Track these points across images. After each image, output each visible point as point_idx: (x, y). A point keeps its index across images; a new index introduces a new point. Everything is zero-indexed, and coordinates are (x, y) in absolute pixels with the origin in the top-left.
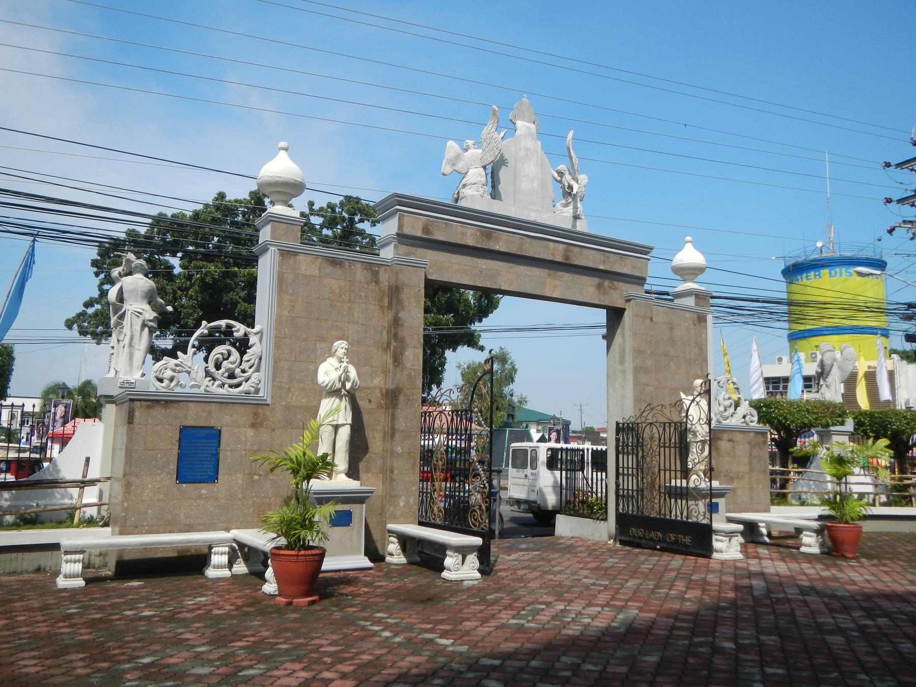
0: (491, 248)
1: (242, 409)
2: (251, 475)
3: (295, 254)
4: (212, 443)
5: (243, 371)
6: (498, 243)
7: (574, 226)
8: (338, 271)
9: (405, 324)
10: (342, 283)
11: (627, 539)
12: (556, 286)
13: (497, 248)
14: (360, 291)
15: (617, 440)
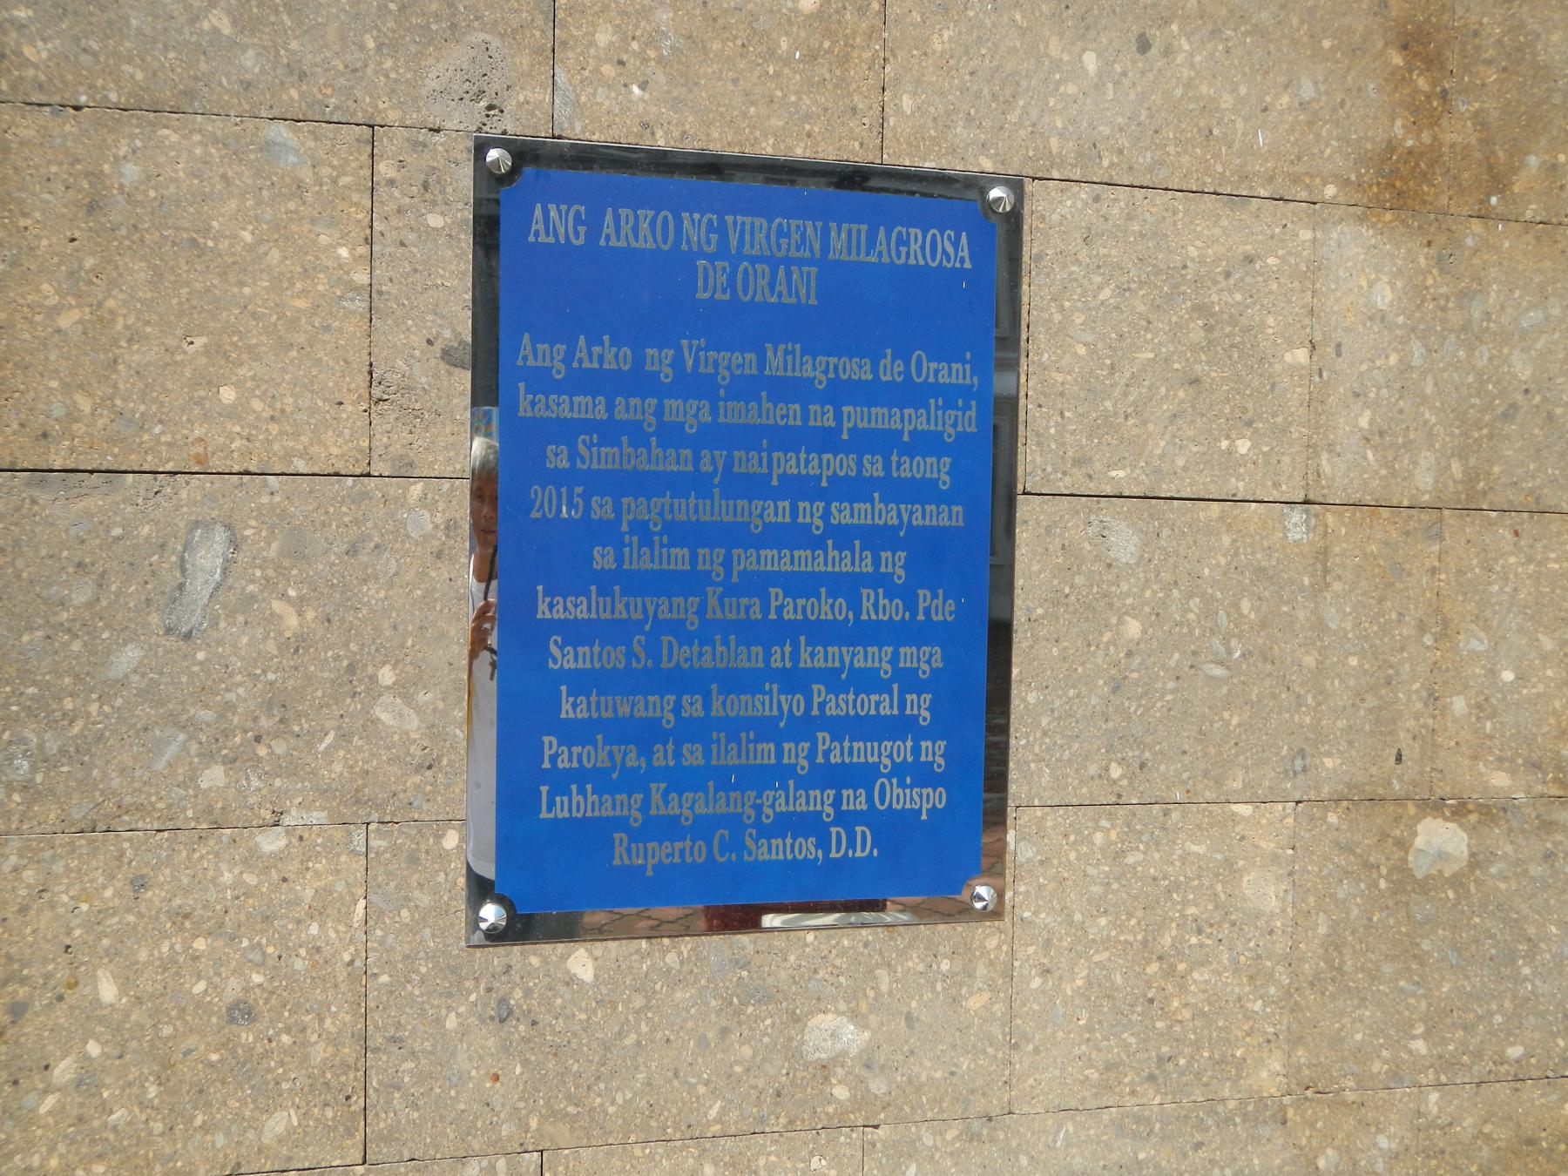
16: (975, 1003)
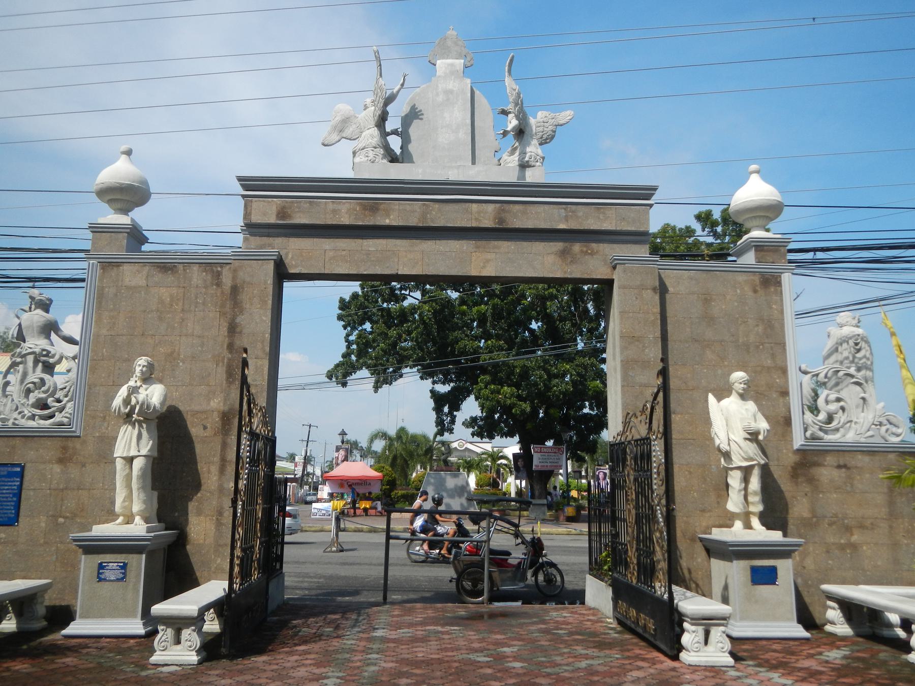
0: (378, 223)
1: (49, 443)
2: (55, 517)
3: (118, 265)
4: (14, 481)
5: (59, 401)
6: (388, 216)
7: (522, 176)
8: (170, 278)
9: (245, 331)
10: (174, 291)
12: (488, 261)
13: (387, 222)
14: (196, 298)
16: (15, 533)
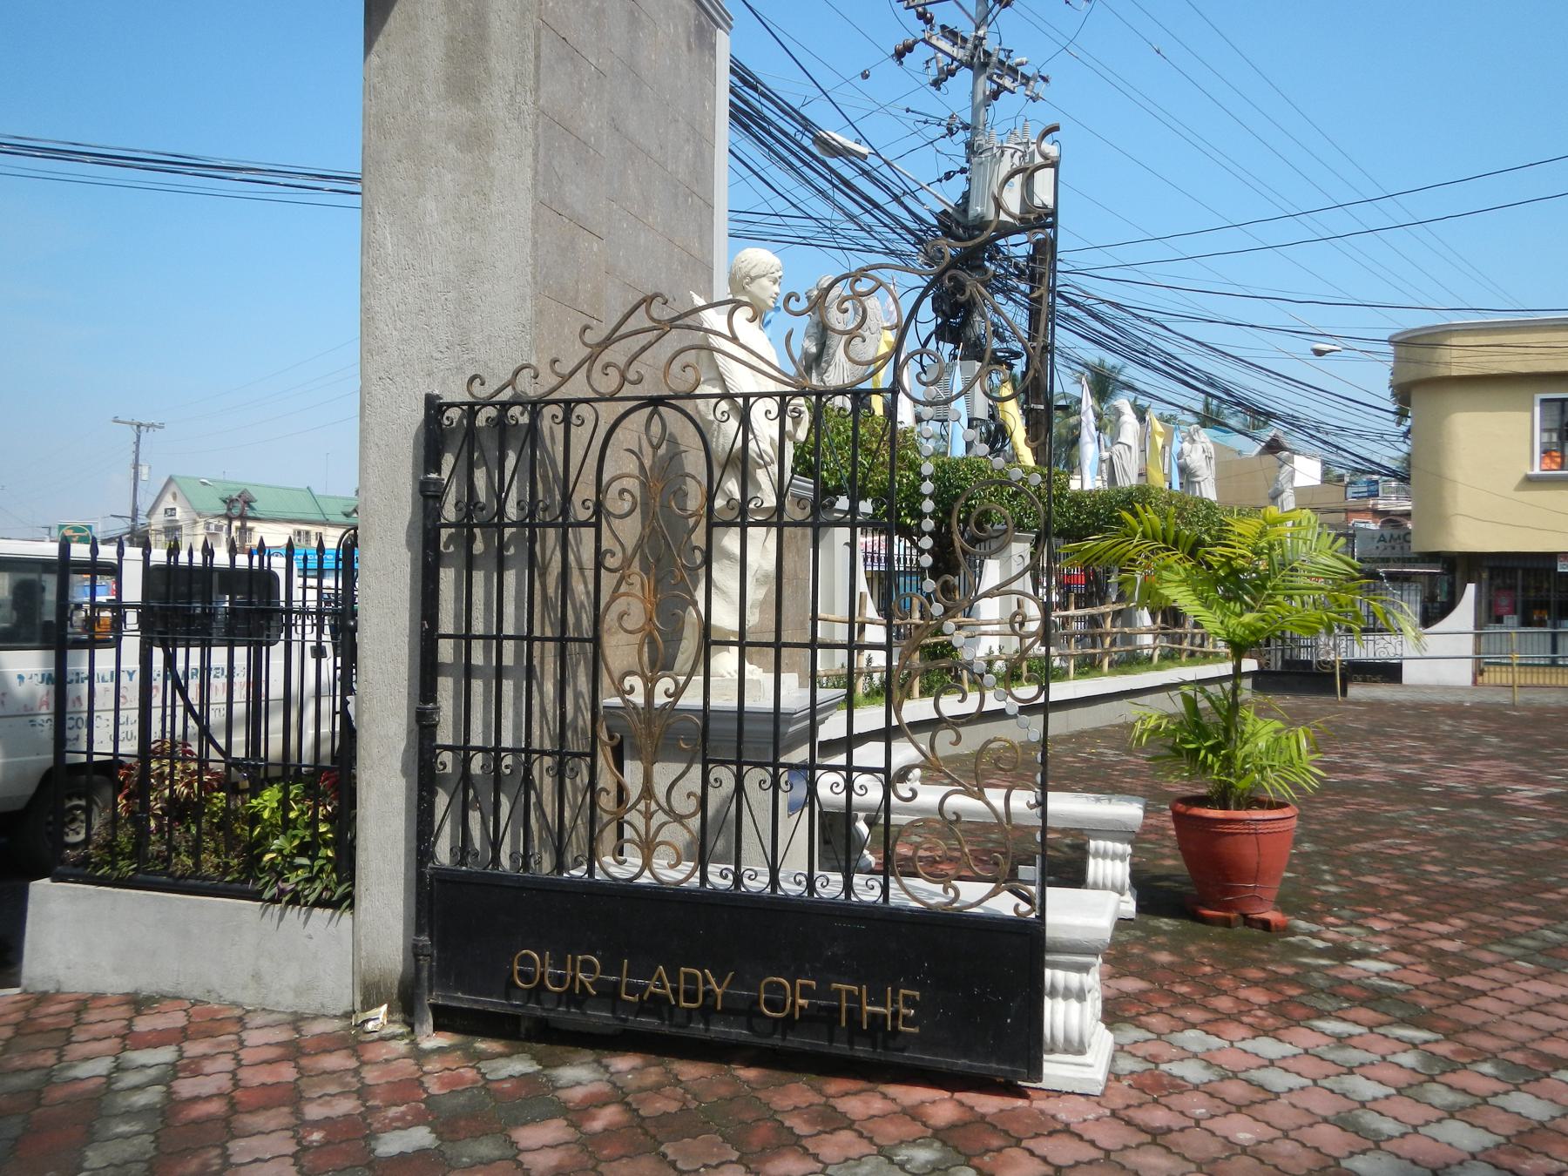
11: (491, 1003)
15: (429, 496)
